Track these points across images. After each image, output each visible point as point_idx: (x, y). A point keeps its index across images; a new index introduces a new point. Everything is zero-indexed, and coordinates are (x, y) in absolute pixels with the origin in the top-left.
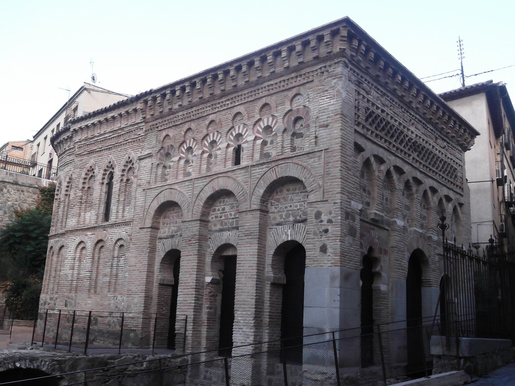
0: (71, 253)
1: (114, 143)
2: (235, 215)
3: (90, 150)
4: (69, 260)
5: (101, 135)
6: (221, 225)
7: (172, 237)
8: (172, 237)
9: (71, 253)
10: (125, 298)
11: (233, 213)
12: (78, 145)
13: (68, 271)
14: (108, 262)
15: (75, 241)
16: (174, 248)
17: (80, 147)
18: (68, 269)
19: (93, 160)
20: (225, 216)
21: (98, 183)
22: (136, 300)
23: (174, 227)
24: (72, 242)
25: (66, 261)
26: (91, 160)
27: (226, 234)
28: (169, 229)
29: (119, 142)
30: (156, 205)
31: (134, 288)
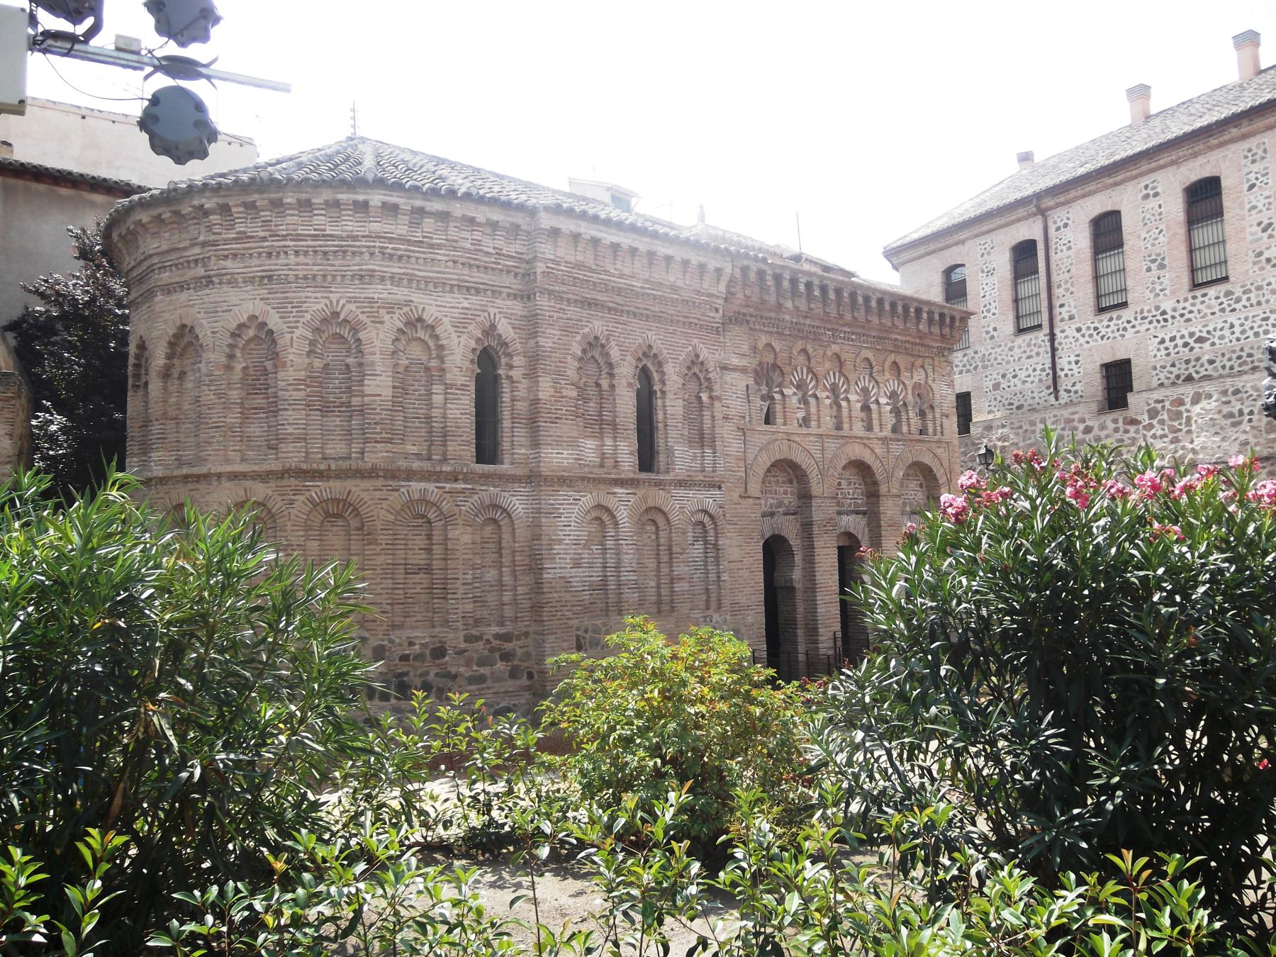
0: (570, 531)
1: (657, 309)
2: (853, 494)
3: (589, 296)
4: (567, 544)
5: (622, 276)
6: (838, 504)
7: (772, 514)
8: (772, 514)
9: (570, 531)
10: (728, 617)
11: (851, 491)
12: (547, 267)
13: (569, 570)
14: (681, 554)
15: (581, 503)
16: (777, 533)
17: (548, 273)
18: (569, 566)
19: (600, 324)
20: (842, 493)
21: (624, 382)
22: (750, 619)
23: (773, 498)
24: (568, 504)
25: (557, 547)
26: (595, 322)
27: (845, 518)
28: (766, 502)
29: (669, 312)
30: (765, 461)
31: (743, 600)
